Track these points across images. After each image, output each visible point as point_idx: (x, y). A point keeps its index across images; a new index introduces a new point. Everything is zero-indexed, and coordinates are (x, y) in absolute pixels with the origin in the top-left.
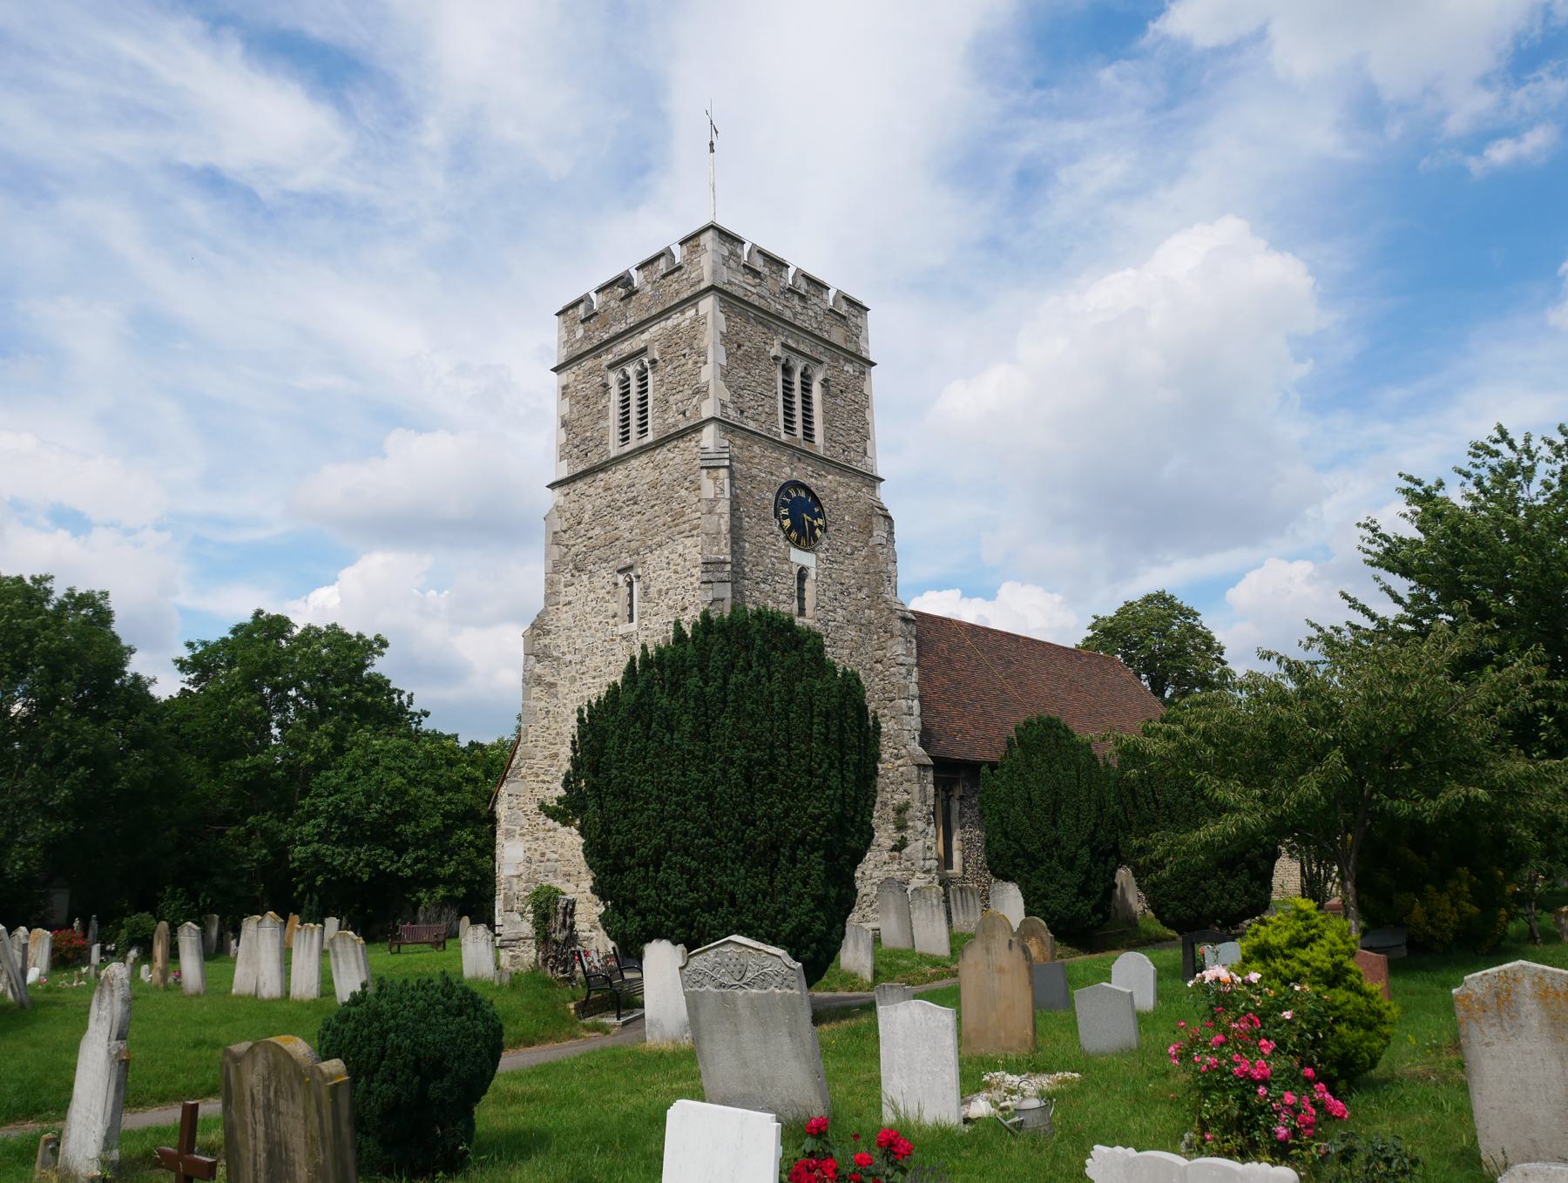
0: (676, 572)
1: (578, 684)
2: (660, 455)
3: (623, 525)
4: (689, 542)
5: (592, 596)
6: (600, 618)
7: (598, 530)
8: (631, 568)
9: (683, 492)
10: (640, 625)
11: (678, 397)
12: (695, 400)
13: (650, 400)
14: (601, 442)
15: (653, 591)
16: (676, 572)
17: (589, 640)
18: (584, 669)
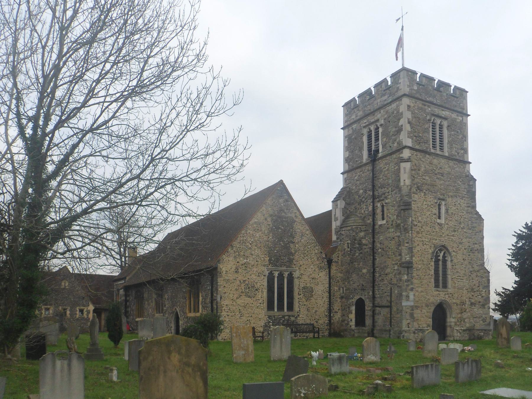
0: (457, 209)
1: (420, 235)
2: (451, 163)
3: (437, 181)
4: (462, 201)
5: (425, 203)
6: (429, 213)
7: (427, 178)
8: (443, 200)
9: (459, 182)
10: (445, 222)
11: (456, 146)
12: (462, 151)
13: (446, 141)
14: (427, 142)
15: (450, 212)
16: (457, 209)
17: (425, 220)
18: (422, 230)
